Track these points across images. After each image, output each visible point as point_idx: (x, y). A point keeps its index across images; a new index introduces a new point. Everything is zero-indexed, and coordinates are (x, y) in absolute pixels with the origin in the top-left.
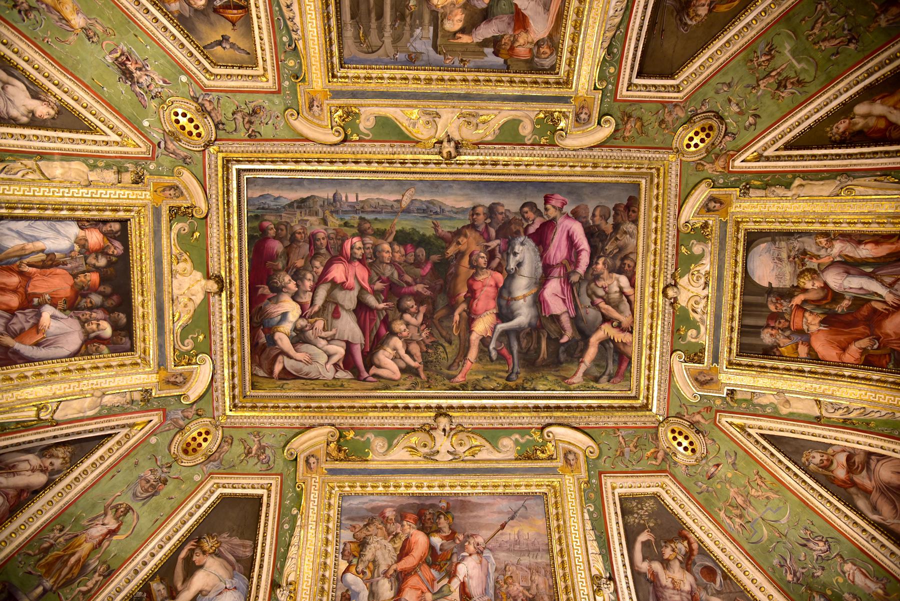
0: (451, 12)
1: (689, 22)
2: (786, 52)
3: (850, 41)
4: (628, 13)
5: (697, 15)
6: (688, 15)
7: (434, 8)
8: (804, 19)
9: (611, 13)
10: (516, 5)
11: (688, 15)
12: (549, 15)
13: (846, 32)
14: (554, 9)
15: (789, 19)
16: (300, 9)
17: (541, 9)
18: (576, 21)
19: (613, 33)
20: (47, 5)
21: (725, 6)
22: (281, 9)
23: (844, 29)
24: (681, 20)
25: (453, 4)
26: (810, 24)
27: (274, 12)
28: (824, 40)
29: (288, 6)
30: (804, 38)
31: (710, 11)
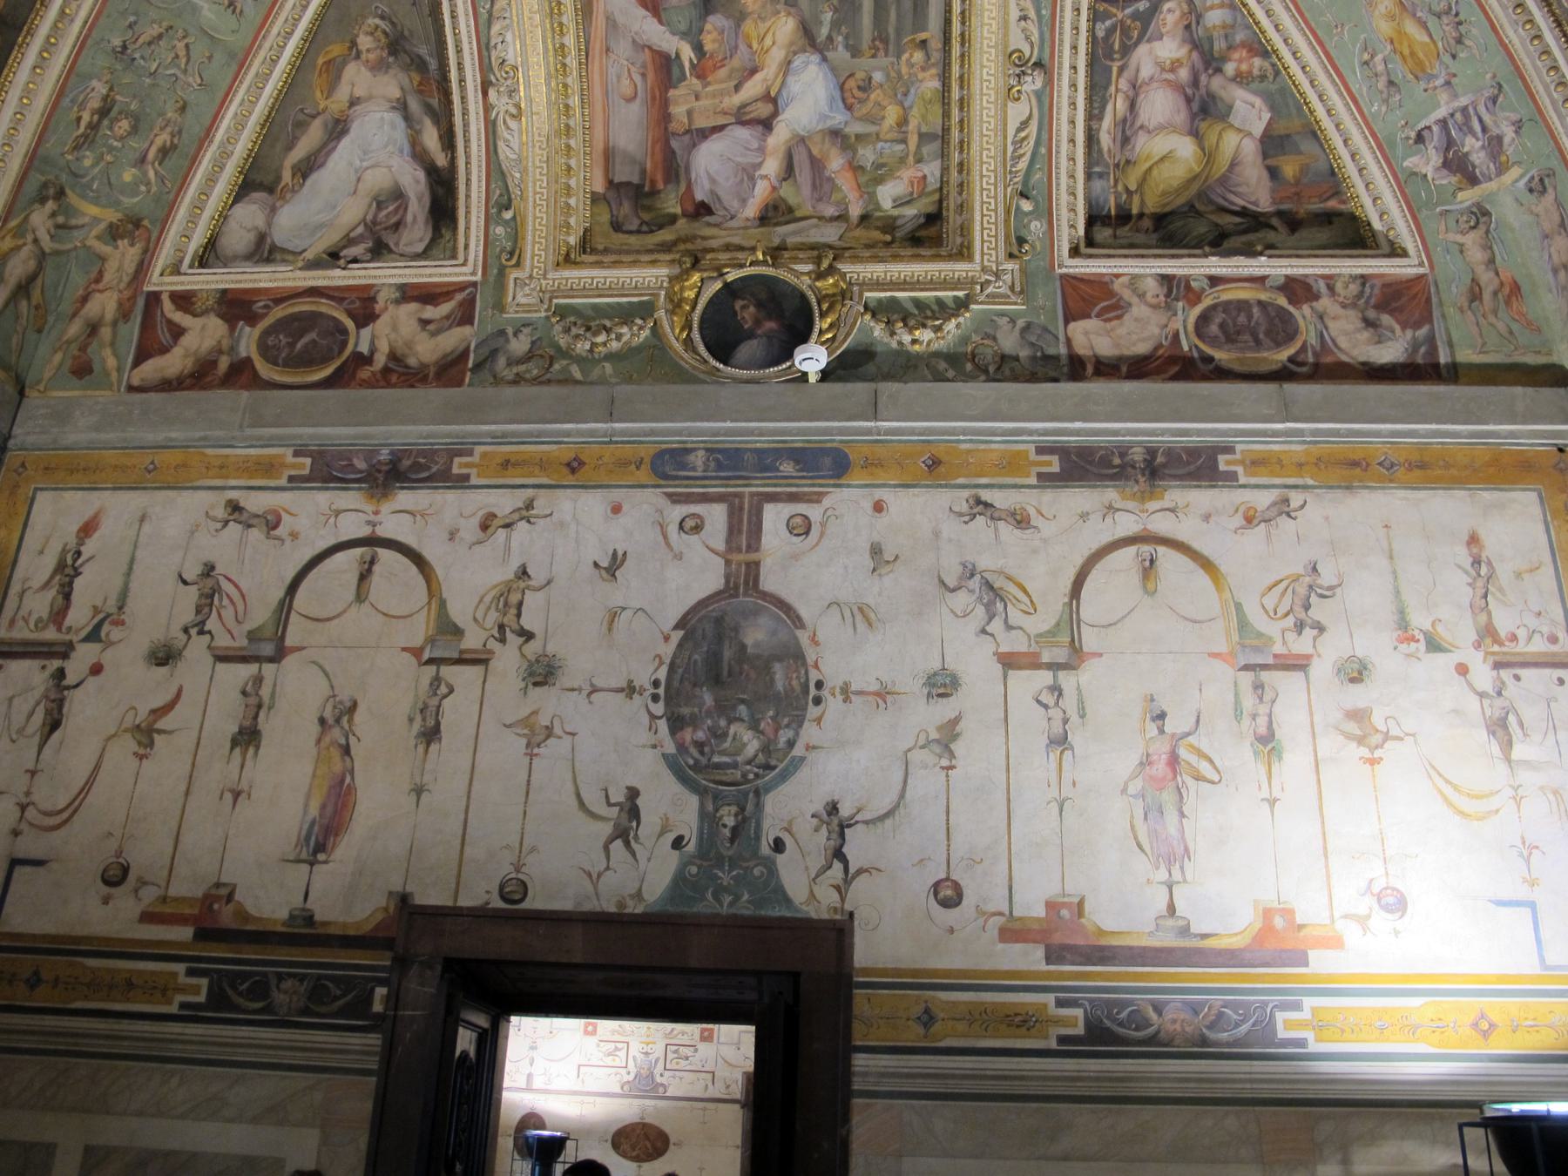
0: (764, 6)
1: (378, 21)
2: (206, 6)
3: (124, 47)
4: (484, 40)
5: (372, 34)
6: (385, 32)
7: (792, 10)
8: (210, 58)
9: (509, 37)
10: (661, 22)
11: (385, 32)
12: (605, 11)
13: (137, 55)
14: (599, 23)
15: (232, 55)
16: (1006, 13)
17: (620, 20)
18: (560, 14)
19: (496, 7)
20: (1414, 15)
21: (335, 54)
22: (1038, 12)
23: (142, 58)
24: (393, 23)
25: (763, 19)
26: (194, 54)
27: (1050, 7)
28: (160, 36)
29: (1024, 18)
30: (191, 30)
31: (354, 44)
